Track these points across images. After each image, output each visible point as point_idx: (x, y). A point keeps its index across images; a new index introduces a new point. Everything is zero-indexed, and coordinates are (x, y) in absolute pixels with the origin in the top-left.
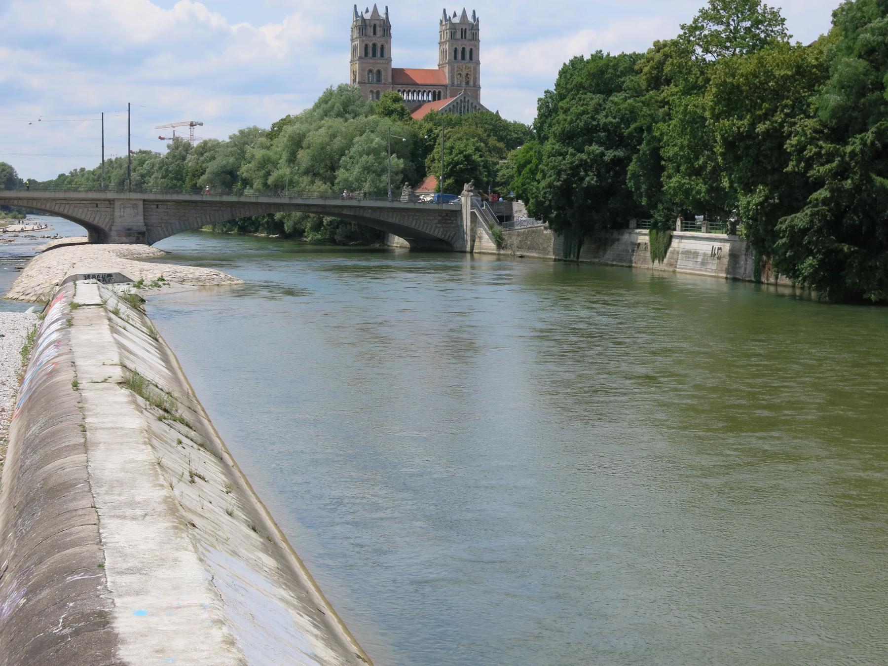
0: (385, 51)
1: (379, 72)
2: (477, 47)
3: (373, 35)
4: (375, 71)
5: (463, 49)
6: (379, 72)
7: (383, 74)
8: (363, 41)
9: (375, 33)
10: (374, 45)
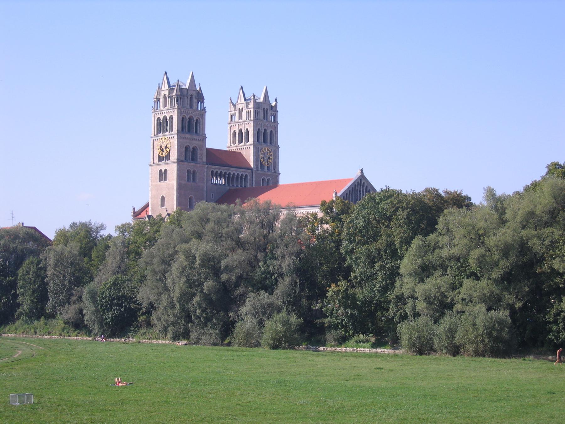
2: (276, 129)
5: (265, 130)
6: (194, 149)
9: (191, 106)
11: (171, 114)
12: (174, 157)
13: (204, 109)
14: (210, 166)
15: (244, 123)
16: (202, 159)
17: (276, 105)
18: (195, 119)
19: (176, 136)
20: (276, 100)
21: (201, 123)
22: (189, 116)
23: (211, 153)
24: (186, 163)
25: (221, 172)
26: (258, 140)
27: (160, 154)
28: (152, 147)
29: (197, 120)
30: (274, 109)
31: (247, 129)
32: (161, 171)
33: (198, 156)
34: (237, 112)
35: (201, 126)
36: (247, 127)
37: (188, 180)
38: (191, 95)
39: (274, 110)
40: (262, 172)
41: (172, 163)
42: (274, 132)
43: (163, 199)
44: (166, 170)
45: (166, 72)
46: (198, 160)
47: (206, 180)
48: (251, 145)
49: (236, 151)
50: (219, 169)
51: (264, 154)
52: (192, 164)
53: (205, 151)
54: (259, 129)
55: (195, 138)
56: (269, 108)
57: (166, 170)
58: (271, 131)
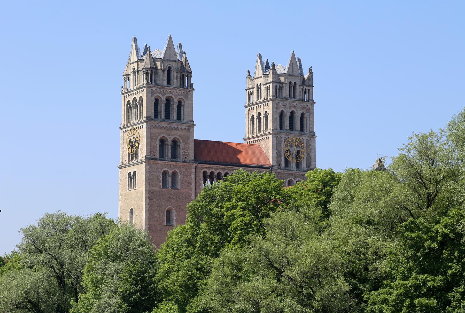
0: (185, 111)
1: (175, 143)
2: (310, 111)
3: (167, 86)
4: (170, 140)
5: (292, 113)
7: (182, 145)
8: (152, 93)
9: (169, 82)
10: (168, 100)
11: (141, 95)
12: (143, 154)
13: (191, 85)
14: (200, 165)
15: (262, 104)
16: (186, 155)
17: (310, 78)
18: (176, 100)
19: (145, 125)
20: (310, 69)
21: (186, 105)
22: (166, 96)
23: (201, 145)
24: (162, 162)
25: (219, 174)
26: (281, 127)
27: (130, 152)
28: (121, 142)
29: (180, 102)
30: (306, 83)
31: (266, 112)
32: (130, 173)
33: (181, 151)
34: (255, 90)
35: (186, 110)
36: (266, 110)
37: (165, 185)
38: (169, 68)
39: (307, 84)
40: (286, 172)
41: (141, 163)
42: (307, 114)
43: (132, 211)
44: (135, 173)
45: (135, 39)
46: (182, 157)
47: (193, 184)
48: (269, 134)
49: (255, 143)
50: (216, 169)
51: (291, 146)
52: (170, 163)
53: (192, 145)
54: (282, 112)
55: (176, 126)
56: (298, 82)
57: (135, 173)
58: (303, 114)
